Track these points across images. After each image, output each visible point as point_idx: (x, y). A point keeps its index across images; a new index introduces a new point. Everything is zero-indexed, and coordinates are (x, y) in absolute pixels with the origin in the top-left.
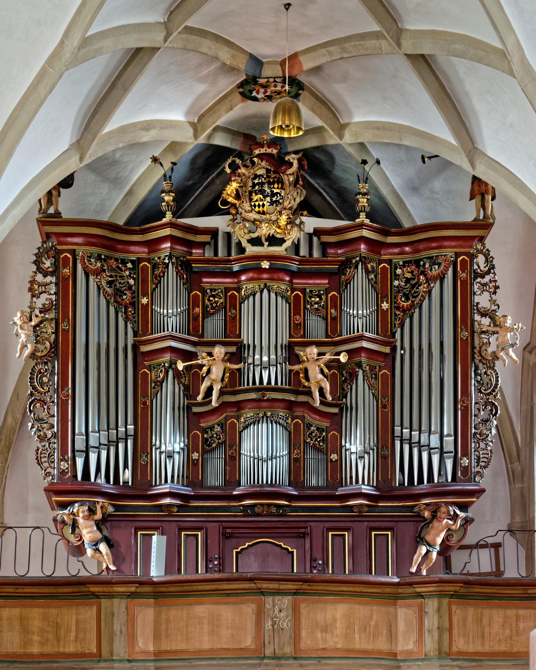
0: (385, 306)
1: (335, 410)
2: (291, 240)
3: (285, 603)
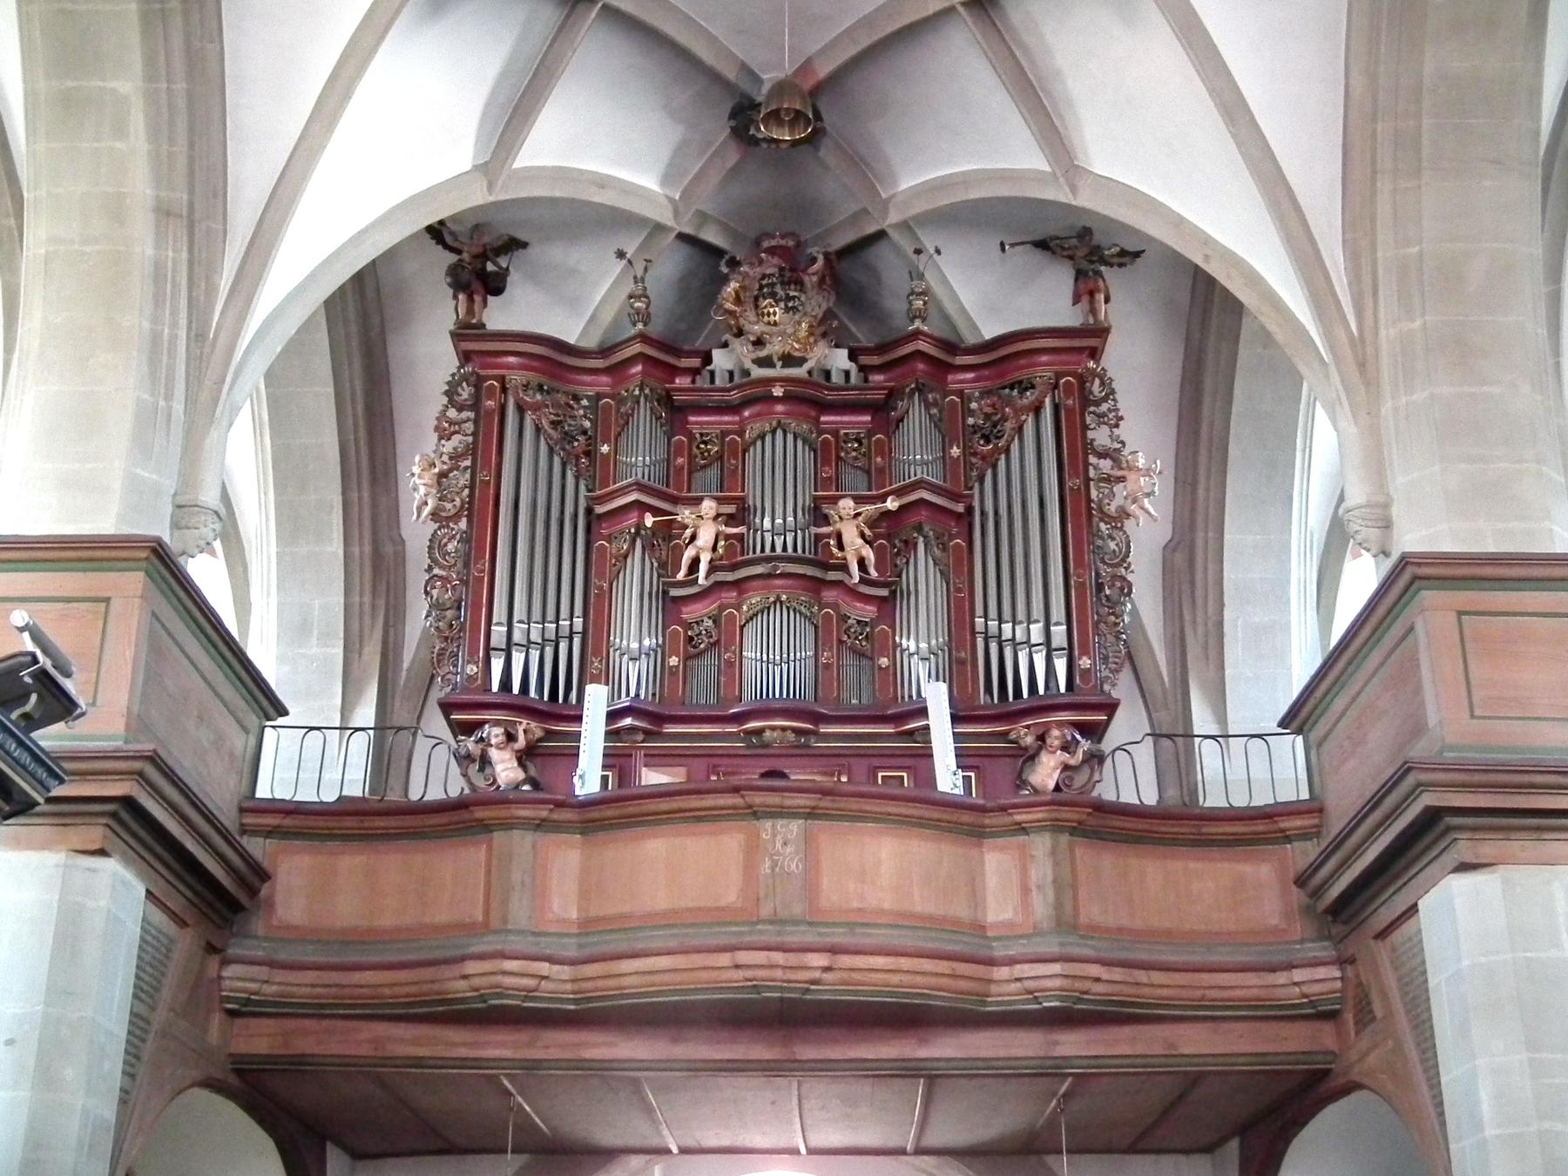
0: (955, 451)
1: (884, 592)
2: (816, 358)
3: (792, 831)
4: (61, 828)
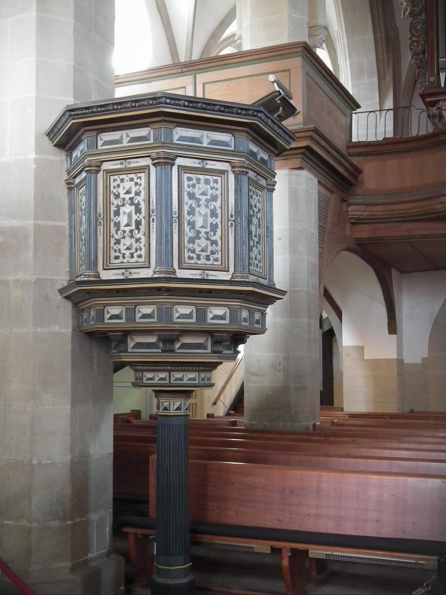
4: (285, 161)
